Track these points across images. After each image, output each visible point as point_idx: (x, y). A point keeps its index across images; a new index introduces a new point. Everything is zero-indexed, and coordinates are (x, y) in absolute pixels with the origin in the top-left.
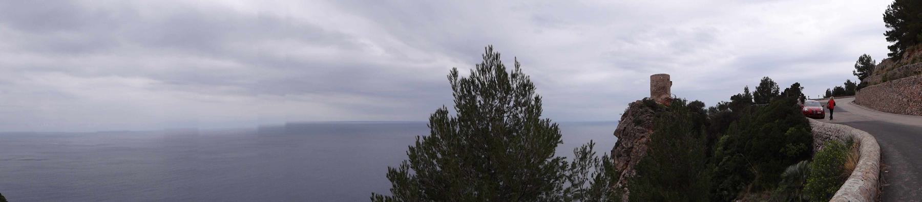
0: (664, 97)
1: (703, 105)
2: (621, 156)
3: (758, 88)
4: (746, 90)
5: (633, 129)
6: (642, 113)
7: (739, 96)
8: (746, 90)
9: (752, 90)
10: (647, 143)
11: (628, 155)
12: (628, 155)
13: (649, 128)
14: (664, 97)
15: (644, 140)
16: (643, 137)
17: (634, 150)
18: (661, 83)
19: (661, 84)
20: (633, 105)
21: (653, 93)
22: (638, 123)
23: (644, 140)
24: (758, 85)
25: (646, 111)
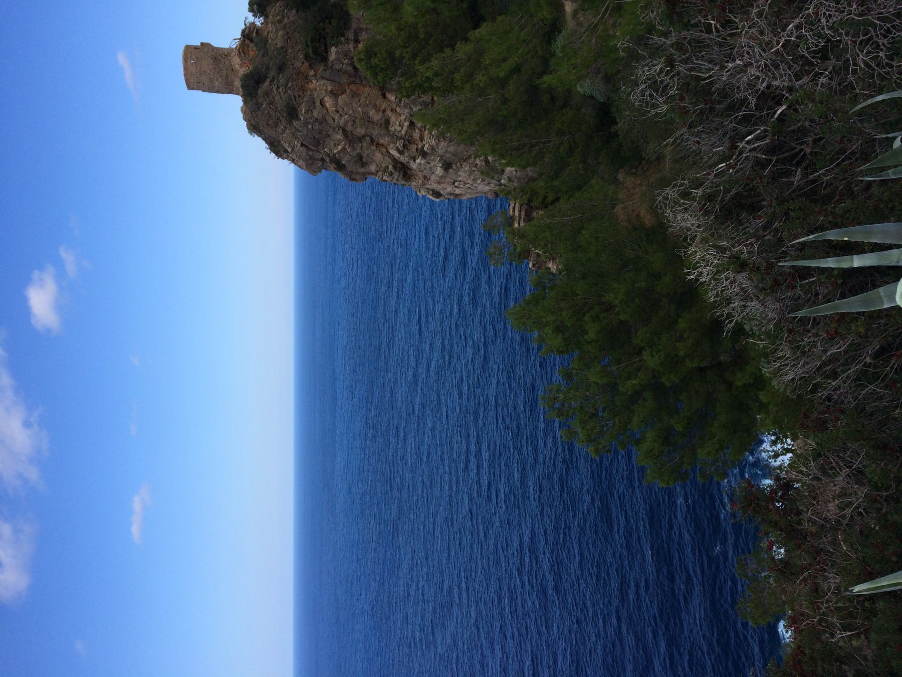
0: (236, 61)
2: (360, 157)
5: (306, 123)
10: (334, 94)
12: (361, 139)
13: (303, 89)
15: (329, 102)
16: (322, 103)
20: (254, 128)
21: (228, 89)
22: (292, 113)
23: (329, 102)
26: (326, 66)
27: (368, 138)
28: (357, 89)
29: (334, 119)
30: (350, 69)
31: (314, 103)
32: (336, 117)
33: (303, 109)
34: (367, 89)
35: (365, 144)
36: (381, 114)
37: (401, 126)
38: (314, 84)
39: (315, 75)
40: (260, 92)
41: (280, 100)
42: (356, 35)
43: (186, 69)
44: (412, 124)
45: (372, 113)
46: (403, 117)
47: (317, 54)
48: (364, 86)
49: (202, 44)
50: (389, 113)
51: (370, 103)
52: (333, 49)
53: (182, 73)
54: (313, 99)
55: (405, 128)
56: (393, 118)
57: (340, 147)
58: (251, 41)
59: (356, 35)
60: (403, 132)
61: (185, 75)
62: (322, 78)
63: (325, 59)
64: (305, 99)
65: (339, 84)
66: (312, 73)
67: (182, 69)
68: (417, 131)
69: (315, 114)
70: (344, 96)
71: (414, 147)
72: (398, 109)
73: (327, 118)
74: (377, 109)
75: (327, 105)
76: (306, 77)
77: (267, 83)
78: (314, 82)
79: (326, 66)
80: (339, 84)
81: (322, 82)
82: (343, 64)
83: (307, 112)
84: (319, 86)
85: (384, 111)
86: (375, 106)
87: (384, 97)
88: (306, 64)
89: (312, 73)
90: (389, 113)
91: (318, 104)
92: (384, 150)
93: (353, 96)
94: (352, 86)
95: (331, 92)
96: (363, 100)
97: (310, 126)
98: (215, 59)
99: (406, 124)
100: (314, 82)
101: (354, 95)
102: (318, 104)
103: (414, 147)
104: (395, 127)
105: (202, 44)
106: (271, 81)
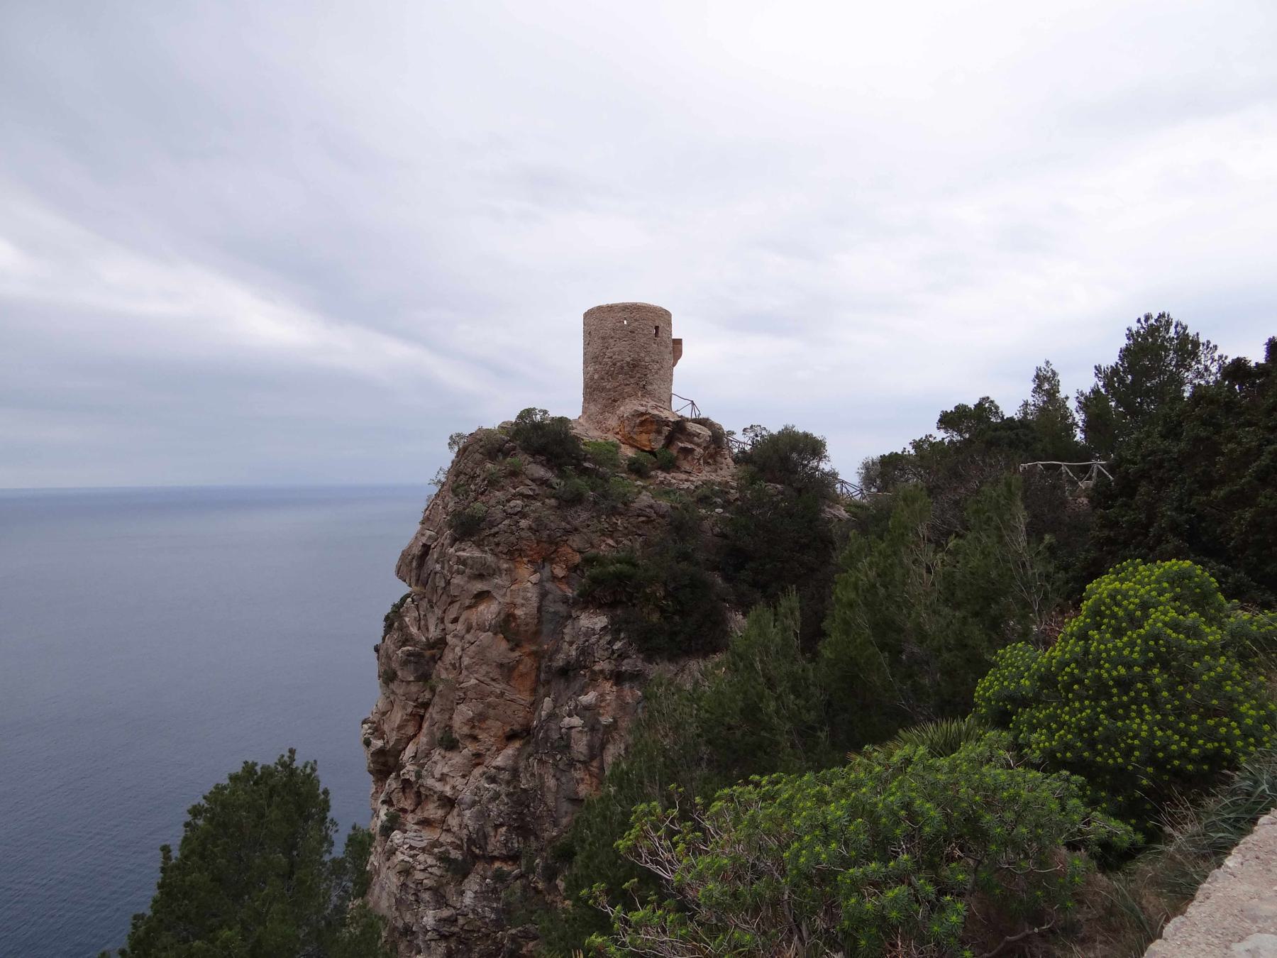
0: (629, 407)
1: (814, 447)
3: (1110, 376)
4: (1046, 382)
6: (493, 483)
7: (984, 409)
8: (1046, 382)
9: (1076, 383)
10: (506, 626)
11: (424, 677)
12: (424, 677)
13: (514, 553)
14: (629, 407)
15: (488, 611)
16: (482, 596)
17: (449, 657)
18: (630, 346)
19: (622, 350)
23: (488, 611)
24: (1111, 358)
25: (514, 474)
26: (575, 603)
27: (428, 695)
28: (521, 675)
29: (455, 620)
30: (560, 660)
31: (480, 577)
32: (460, 627)
33: (469, 552)
34: (525, 697)
35: (414, 688)
36: (466, 730)
37: (443, 778)
38: (528, 577)
39: (554, 578)
40: (522, 459)
41: (495, 503)
42: (636, 677)
43: (611, 308)
44: (449, 803)
45: (465, 711)
46: (459, 782)
47: (606, 589)
48: (534, 691)
49: (678, 342)
50: (469, 749)
51: (489, 705)
52: (600, 621)
53: (603, 302)
54: (492, 575)
55: (439, 786)
56: (457, 758)
57: (414, 630)
58: (670, 440)
59: (636, 677)
60: (430, 782)
61: (600, 308)
62: (543, 595)
63: (588, 601)
64: (490, 558)
65: (537, 633)
66: (559, 571)
67: (610, 303)
68: (440, 813)
69: (457, 580)
70: (504, 645)
71: (408, 804)
72: (478, 771)
73: (457, 605)
74: (478, 720)
75: (481, 608)
76: (548, 559)
77: (540, 472)
78: (535, 578)
79: (575, 603)
80: (537, 633)
81: (533, 595)
82: (571, 643)
83: (461, 561)
84: (523, 589)
85: (475, 738)
86: (481, 717)
87: (511, 737)
88: (577, 558)
89: (559, 571)
90: (469, 749)
91: (479, 586)
92: (410, 730)
93: (501, 665)
94: (528, 661)
95: (510, 617)
96: (498, 688)
97: (438, 567)
98: (635, 365)
99: (448, 791)
100: (535, 578)
101: (507, 671)
102: (479, 586)
103: (408, 804)
104: (442, 763)
105: (678, 342)
106: (543, 482)
